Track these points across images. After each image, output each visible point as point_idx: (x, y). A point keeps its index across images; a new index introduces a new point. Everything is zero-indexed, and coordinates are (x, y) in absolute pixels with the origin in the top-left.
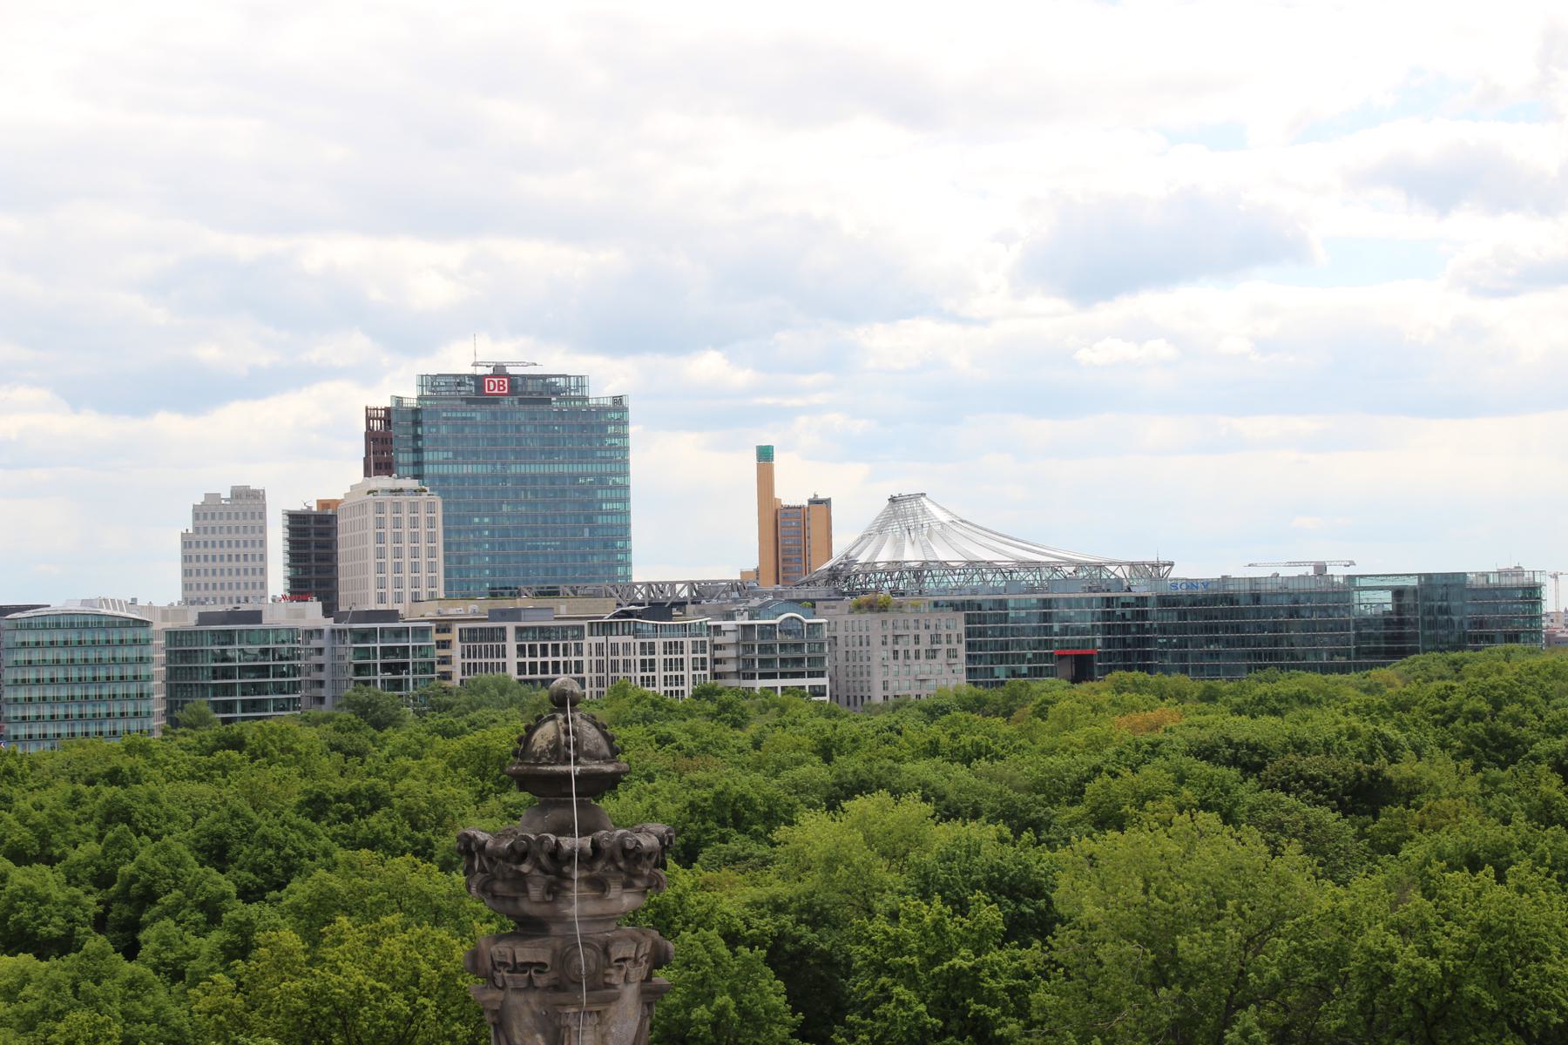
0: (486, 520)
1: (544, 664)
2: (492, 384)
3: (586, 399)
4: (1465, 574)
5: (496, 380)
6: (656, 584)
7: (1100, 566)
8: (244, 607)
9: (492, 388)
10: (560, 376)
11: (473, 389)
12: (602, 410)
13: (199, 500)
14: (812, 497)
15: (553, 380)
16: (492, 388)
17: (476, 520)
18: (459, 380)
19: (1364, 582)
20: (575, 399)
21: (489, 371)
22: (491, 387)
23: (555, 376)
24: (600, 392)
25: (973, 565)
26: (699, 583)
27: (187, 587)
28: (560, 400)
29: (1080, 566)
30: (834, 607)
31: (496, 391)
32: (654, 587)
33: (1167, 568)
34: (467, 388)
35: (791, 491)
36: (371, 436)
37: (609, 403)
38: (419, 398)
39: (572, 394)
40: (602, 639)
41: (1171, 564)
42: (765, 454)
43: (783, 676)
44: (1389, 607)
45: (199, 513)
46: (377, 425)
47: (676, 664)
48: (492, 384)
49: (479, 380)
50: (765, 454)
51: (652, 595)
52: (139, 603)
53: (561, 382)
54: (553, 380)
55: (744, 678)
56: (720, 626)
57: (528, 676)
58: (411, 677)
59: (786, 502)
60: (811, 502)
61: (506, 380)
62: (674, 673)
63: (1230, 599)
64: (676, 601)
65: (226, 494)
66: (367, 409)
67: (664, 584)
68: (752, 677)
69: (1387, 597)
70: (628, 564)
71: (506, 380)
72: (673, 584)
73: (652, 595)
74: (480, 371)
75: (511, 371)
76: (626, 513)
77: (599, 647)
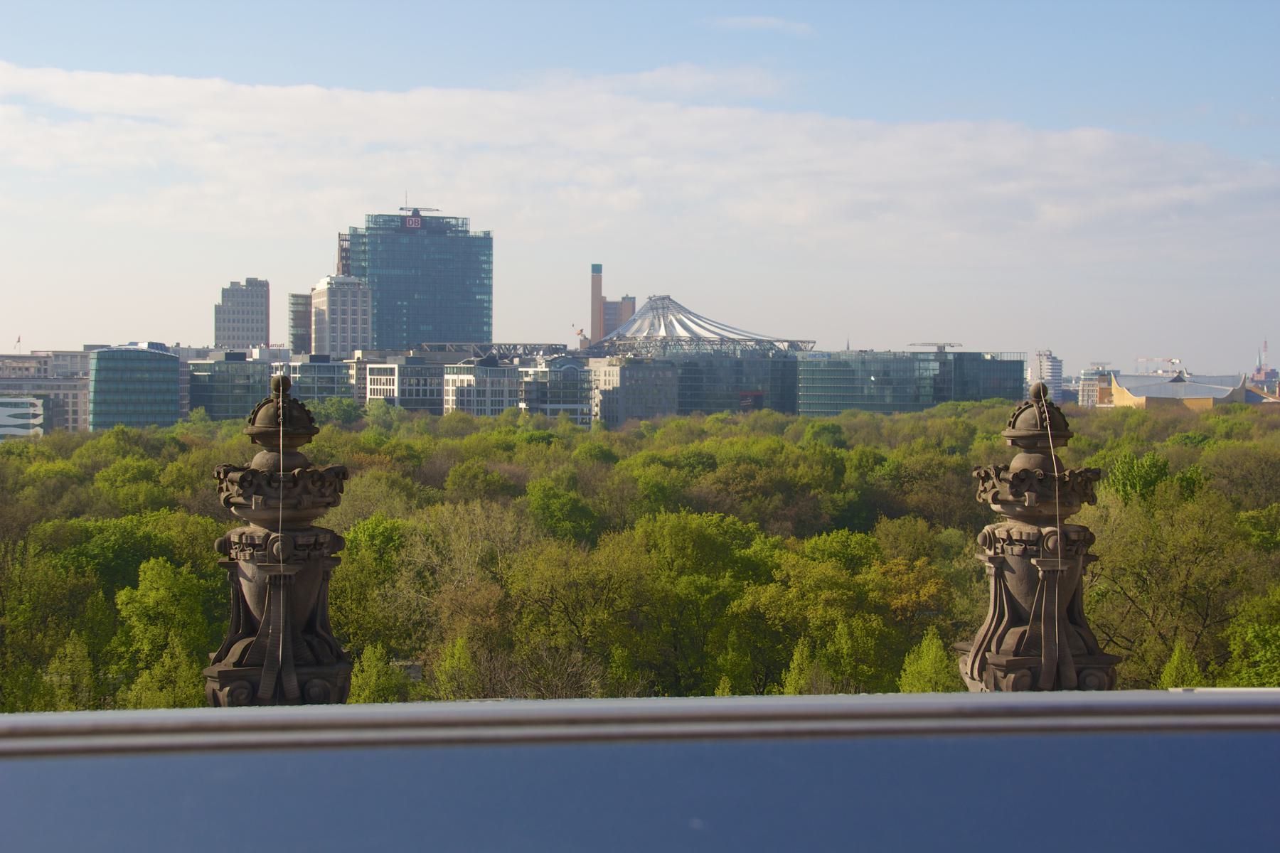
0: (405, 303)
1: (418, 391)
2: (411, 222)
3: (469, 231)
4: (980, 353)
5: (413, 219)
6: (505, 345)
7: (771, 342)
8: (237, 351)
9: (411, 223)
10: (452, 218)
11: (399, 224)
12: (476, 238)
13: (228, 286)
14: (625, 296)
15: (448, 220)
16: (411, 223)
17: (399, 303)
18: (391, 218)
19: (921, 357)
20: (461, 231)
21: (410, 213)
22: (410, 224)
23: (448, 218)
24: (475, 229)
25: (723, 340)
26: (530, 345)
27: (217, 338)
28: (452, 231)
29: (758, 342)
30: (599, 362)
31: (413, 226)
32: (503, 347)
33: (811, 345)
34: (396, 224)
35: (612, 293)
36: (342, 250)
37: (482, 235)
38: (368, 229)
39: (460, 229)
40: (455, 377)
41: (815, 342)
42: (597, 269)
43: (564, 402)
44: (937, 372)
45: (225, 292)
46: (346, 244)
47: (496, 394)
48: (411, 222)
49: (403, 218)
50: (597, 269)
51: (502, 352)
52: (181, 346)
53: (453, 222)
54: (448, 220)
55: (541, 403)
56: (528, 372)
57: (407, 397)
58: (316, 396)
59: (609, 299)
60: (623, 298)
61: (419, 219)
62: (497, 399)
63: (846, 364)
64: (516, 355)
65: (243, 283)
66: (339, 234)
67: (510, 345)
68: (546, 402)
69: (936, 365)
70: (490, 333)
71: (419, 219)
72: (515, 346)
73: (502, 352)
74: (403, 213)
75: (423, 214)
76: (490, 301)
77: (454, 381)
